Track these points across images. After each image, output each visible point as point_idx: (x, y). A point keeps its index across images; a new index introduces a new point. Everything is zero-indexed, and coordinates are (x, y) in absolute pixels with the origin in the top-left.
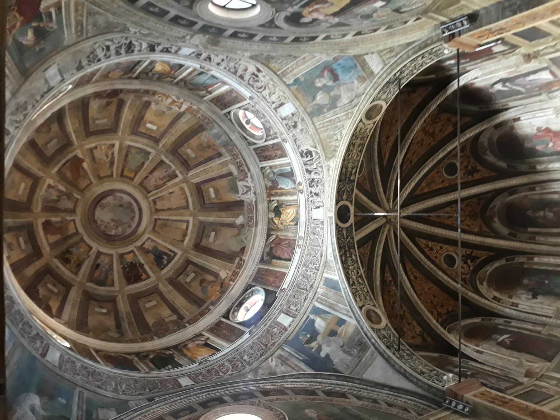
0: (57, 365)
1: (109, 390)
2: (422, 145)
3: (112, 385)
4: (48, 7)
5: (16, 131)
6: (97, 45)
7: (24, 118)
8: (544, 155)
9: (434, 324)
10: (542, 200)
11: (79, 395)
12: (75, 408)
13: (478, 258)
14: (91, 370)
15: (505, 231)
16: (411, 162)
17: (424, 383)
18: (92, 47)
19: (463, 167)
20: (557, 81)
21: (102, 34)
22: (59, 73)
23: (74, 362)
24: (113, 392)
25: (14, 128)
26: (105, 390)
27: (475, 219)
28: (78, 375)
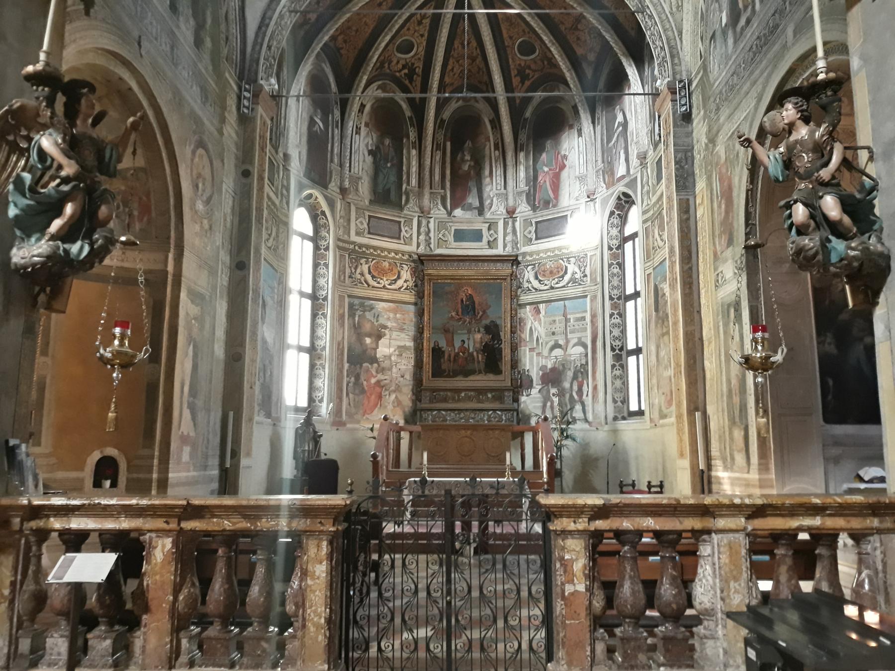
8: (535, 161)
9: (322, 38)
10: (484, 157)
13: (411, 83)
15: (446, 115)
17: (259, 53)
19: (528, 63)
20: (613, 178)
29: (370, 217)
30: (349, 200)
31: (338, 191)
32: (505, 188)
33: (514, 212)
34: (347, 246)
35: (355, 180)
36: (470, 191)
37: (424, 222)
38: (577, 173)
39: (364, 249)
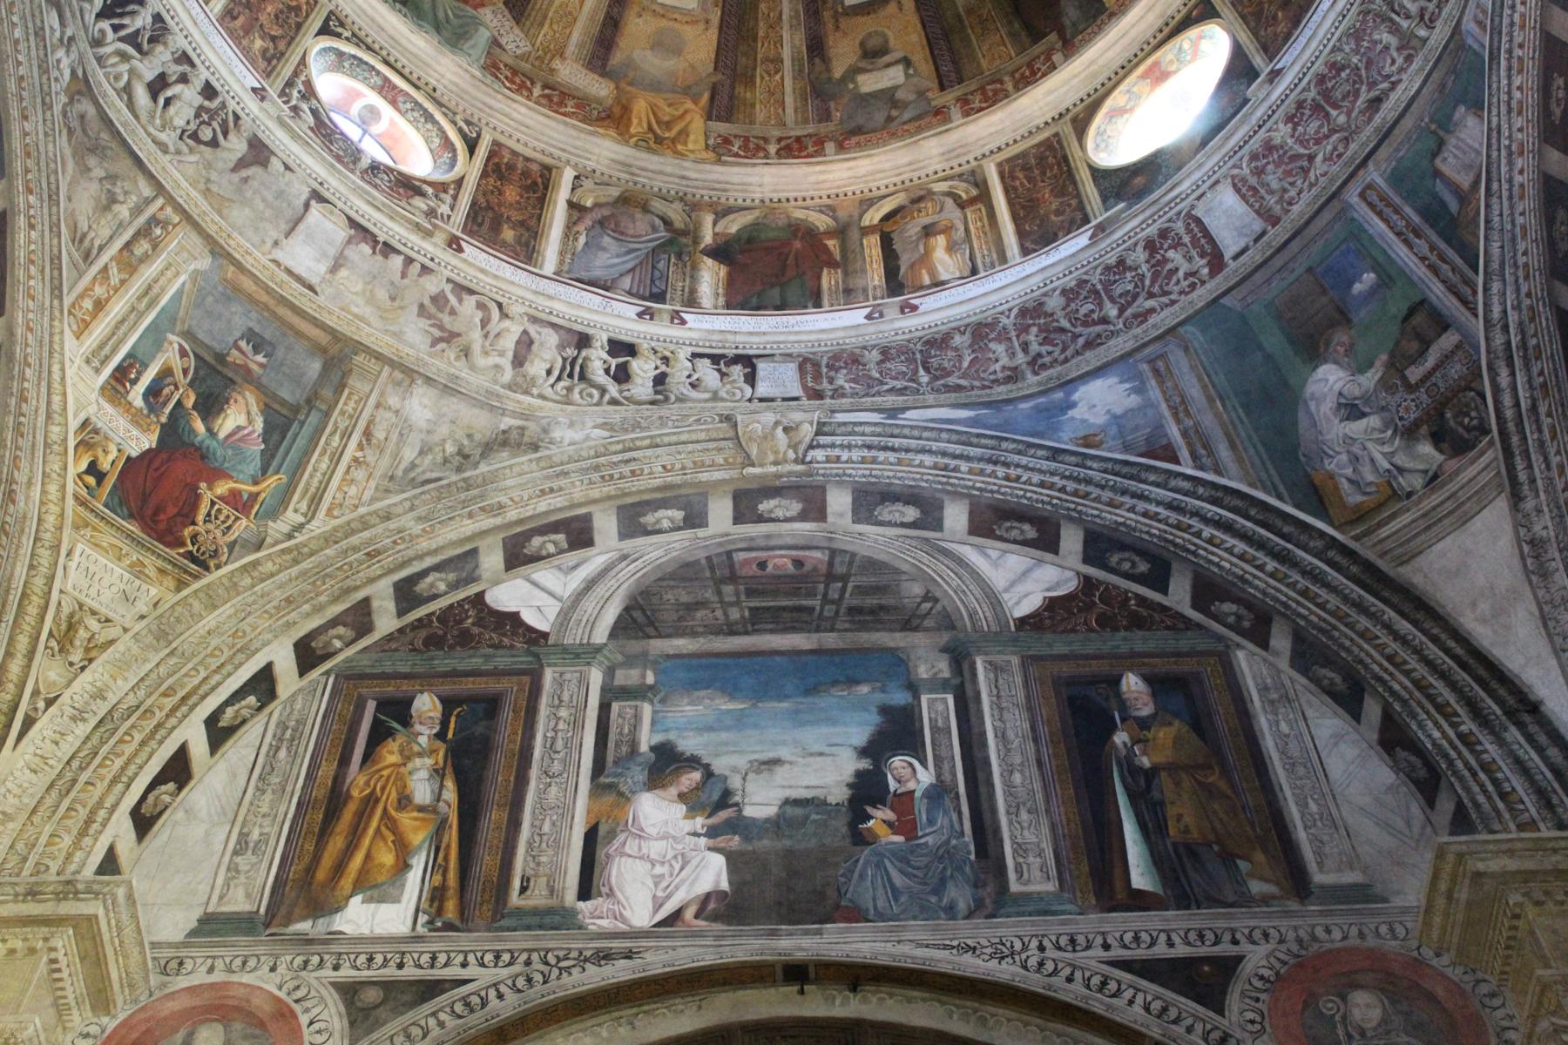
0: (1258, 225)
1: (1401, 70)
3: (1387, 48)
4: (136, 419)
5: (515, 309)
6: (163, 137)
7: (471, 292)
11: (1371, 205)
12: (1401, 252)
14: (1313, 94)
18: (178, 152)
21: (124, 142)
22: (301, 227)
23: (1269, 147)
24: (1409, 59)
25: (507, 323)
26: (1394, 85)
28: (1311, 158)
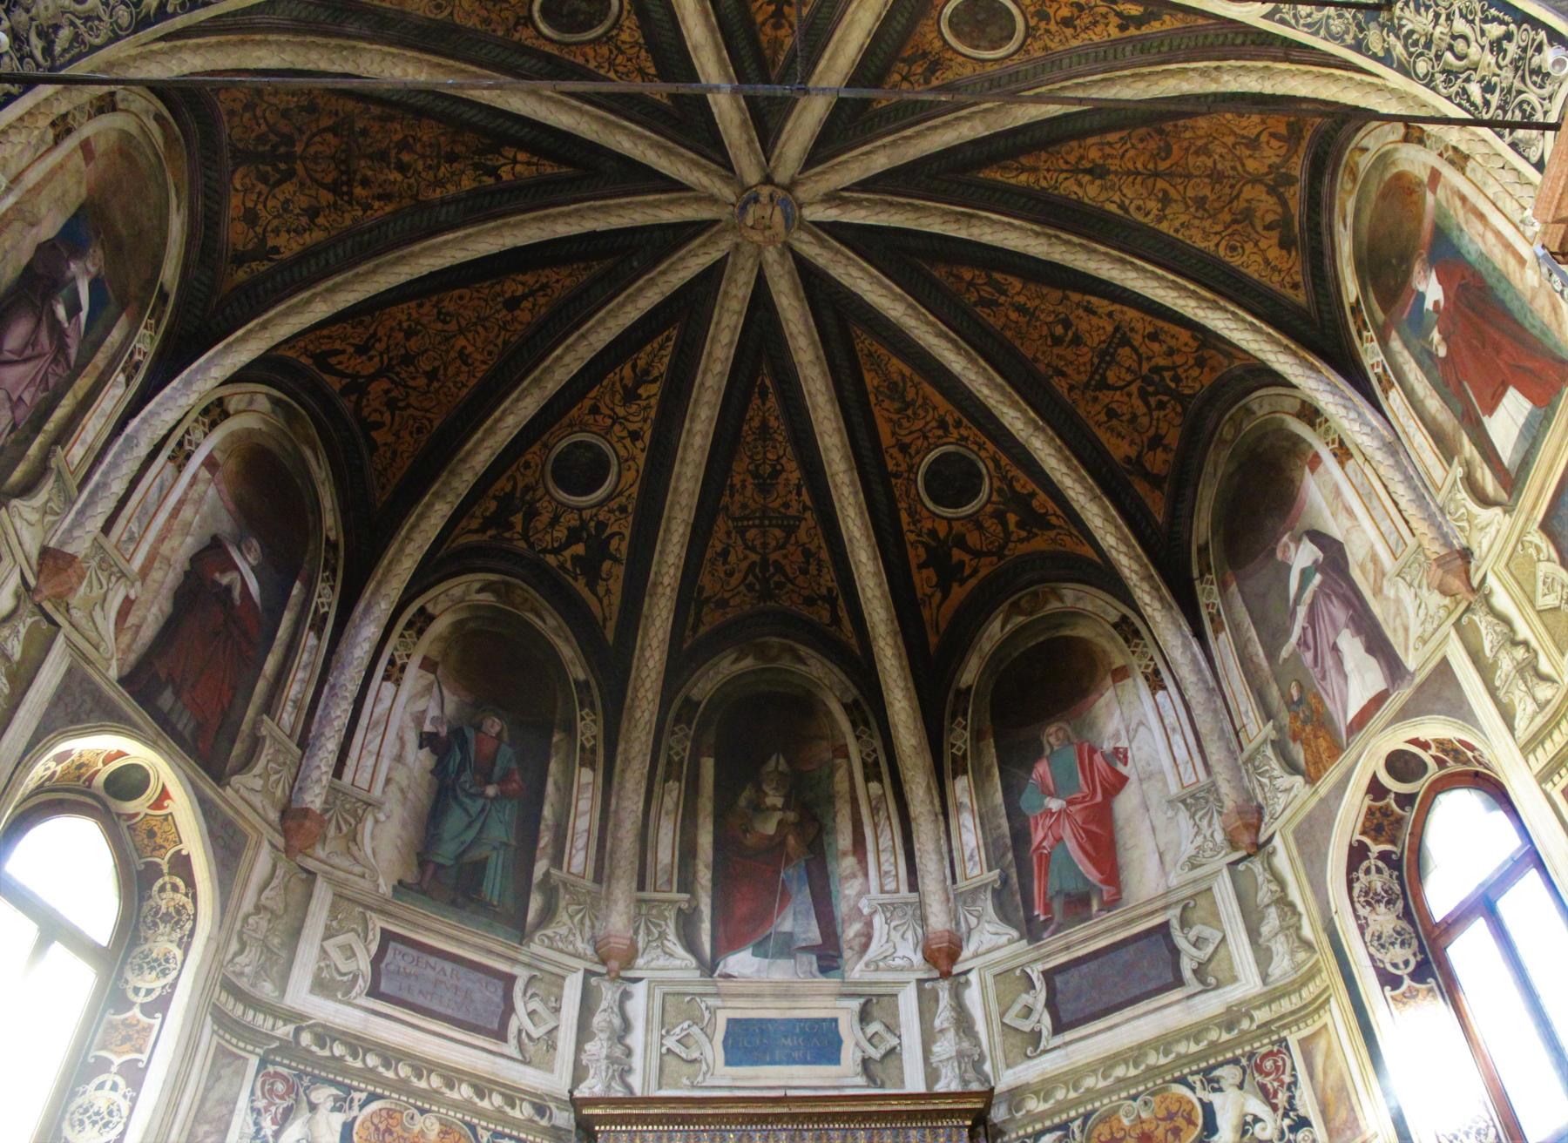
2: (1057, 341)
10: (831, 799)
13: (592, 586)
15: (704, 686)
16: (982, 302)
19: (957, 526)
20: (1333, 734)
27: (750, 587)
29: (387, 937)
30: (311, 864)
31: (274, 816)
32: (913, 886)
33: (953, 953)
34: (263, 1022)
35: (352, 808)
36: (785, 897)
37: (608, 994)
38: (1174, 789)
39: (339, 1050)
